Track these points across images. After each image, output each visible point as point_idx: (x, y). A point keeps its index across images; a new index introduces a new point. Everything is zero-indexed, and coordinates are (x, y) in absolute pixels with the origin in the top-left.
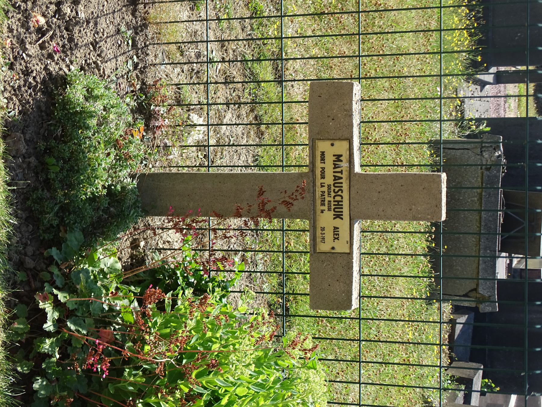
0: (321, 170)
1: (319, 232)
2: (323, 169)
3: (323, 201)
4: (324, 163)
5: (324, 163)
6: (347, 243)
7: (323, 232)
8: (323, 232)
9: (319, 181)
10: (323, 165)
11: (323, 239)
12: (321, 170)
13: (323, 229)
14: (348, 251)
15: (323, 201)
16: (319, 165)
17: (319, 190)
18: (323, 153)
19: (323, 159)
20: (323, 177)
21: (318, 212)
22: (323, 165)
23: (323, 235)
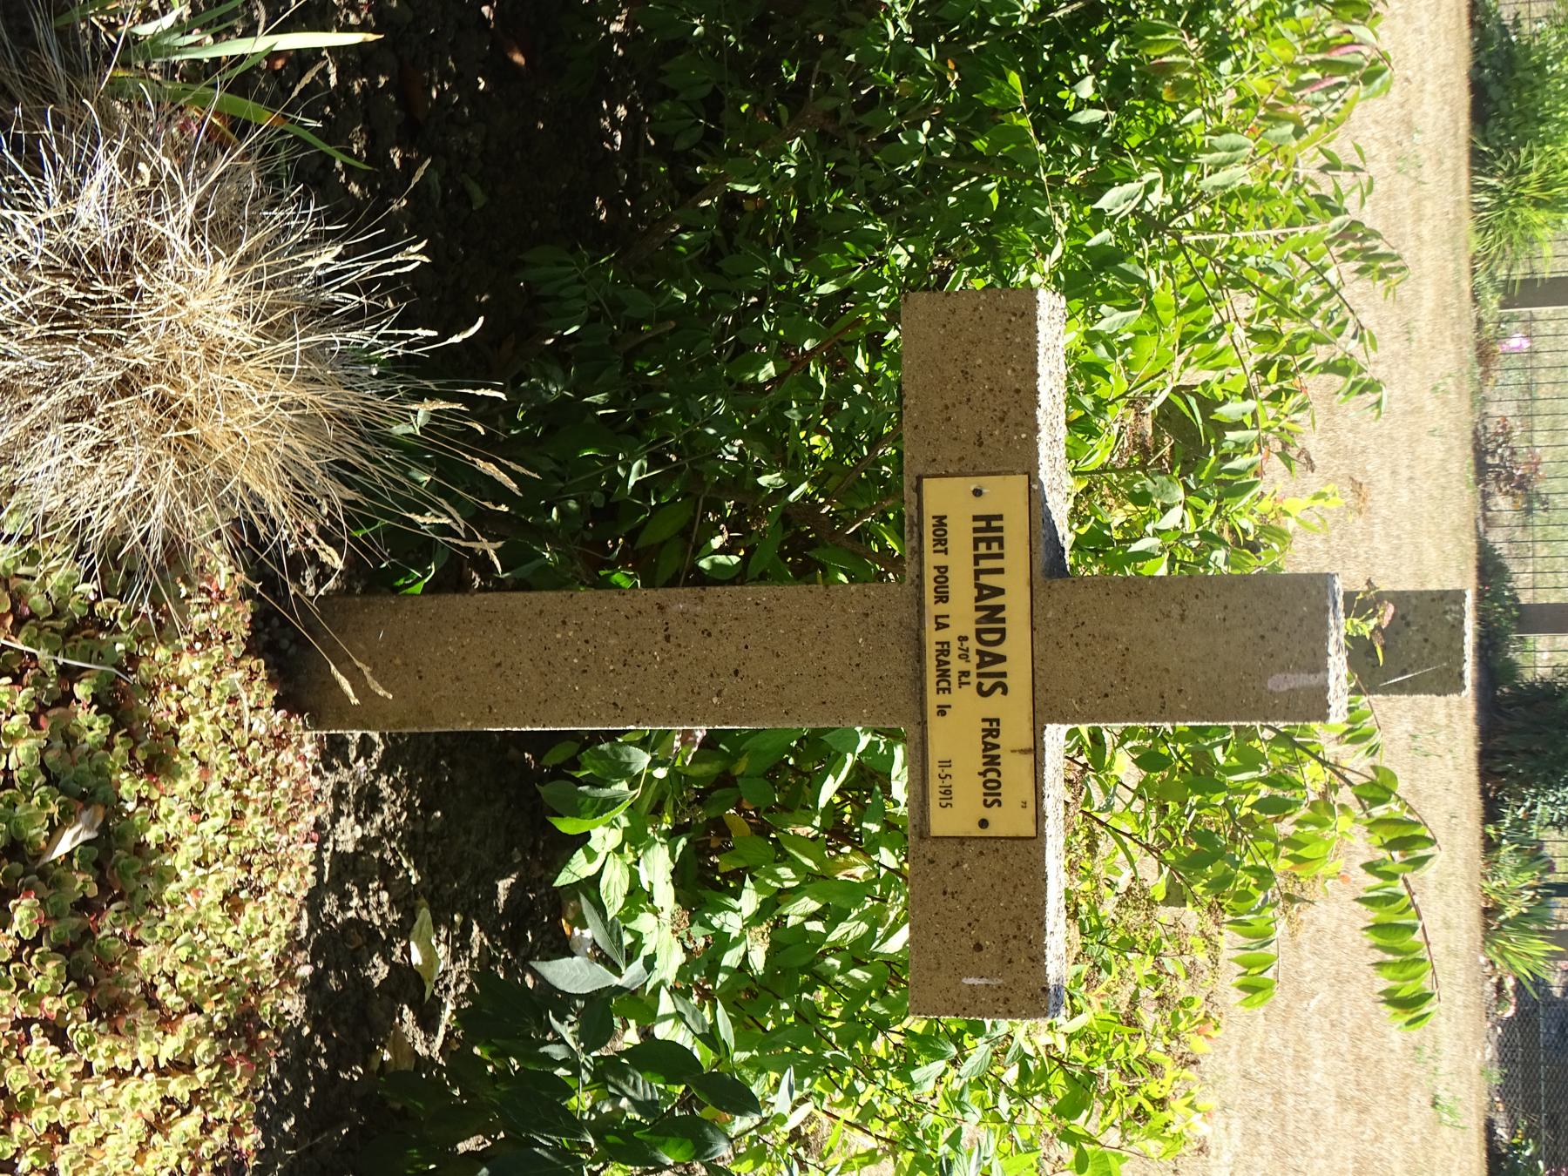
0: (936, 573)
1: (934, 769)
2: (942, 570)
3: (944, 675)
4: (946, 551)
5: (946, 551)
6: (1024, 805)
7: (947, 771)
8: (947, 771)
9: (932, 608)
10: (940, 560)
11: (947, 792)
12: (936, 573)
13: (946, 764)
14: (1031, 832)
15: (944, 675)
16: (931, 559)
17: (932, 637)
18: (941, 521)
19: (941, 541)
20: (942, 598)
21: (931, 710)
22: (940, 560)
23: (947, 782)
